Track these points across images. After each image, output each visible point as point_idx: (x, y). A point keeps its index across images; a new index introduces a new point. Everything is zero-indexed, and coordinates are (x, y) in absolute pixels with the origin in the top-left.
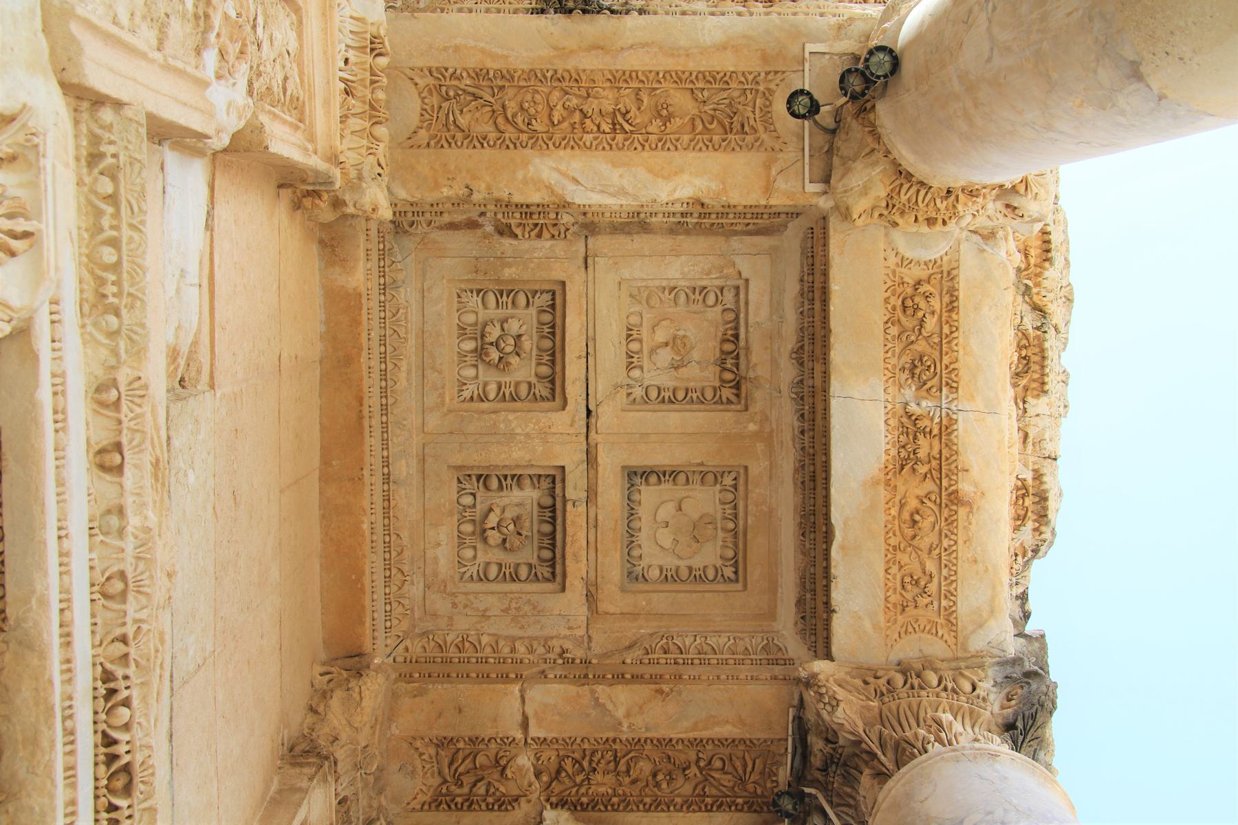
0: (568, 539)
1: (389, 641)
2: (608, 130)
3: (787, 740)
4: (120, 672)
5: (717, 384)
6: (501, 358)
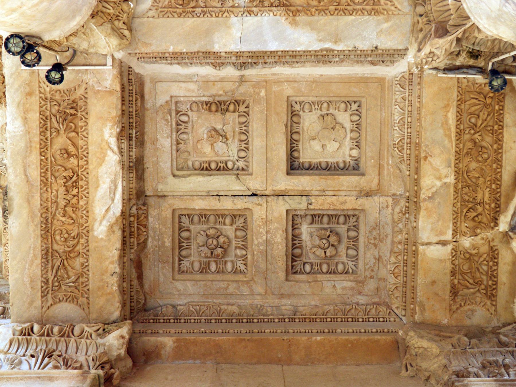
0: (332, 207)
1: (392, 319)
2: (77, 190)
3: (458, 78)
5: (237, 114)
6: (221, 247)
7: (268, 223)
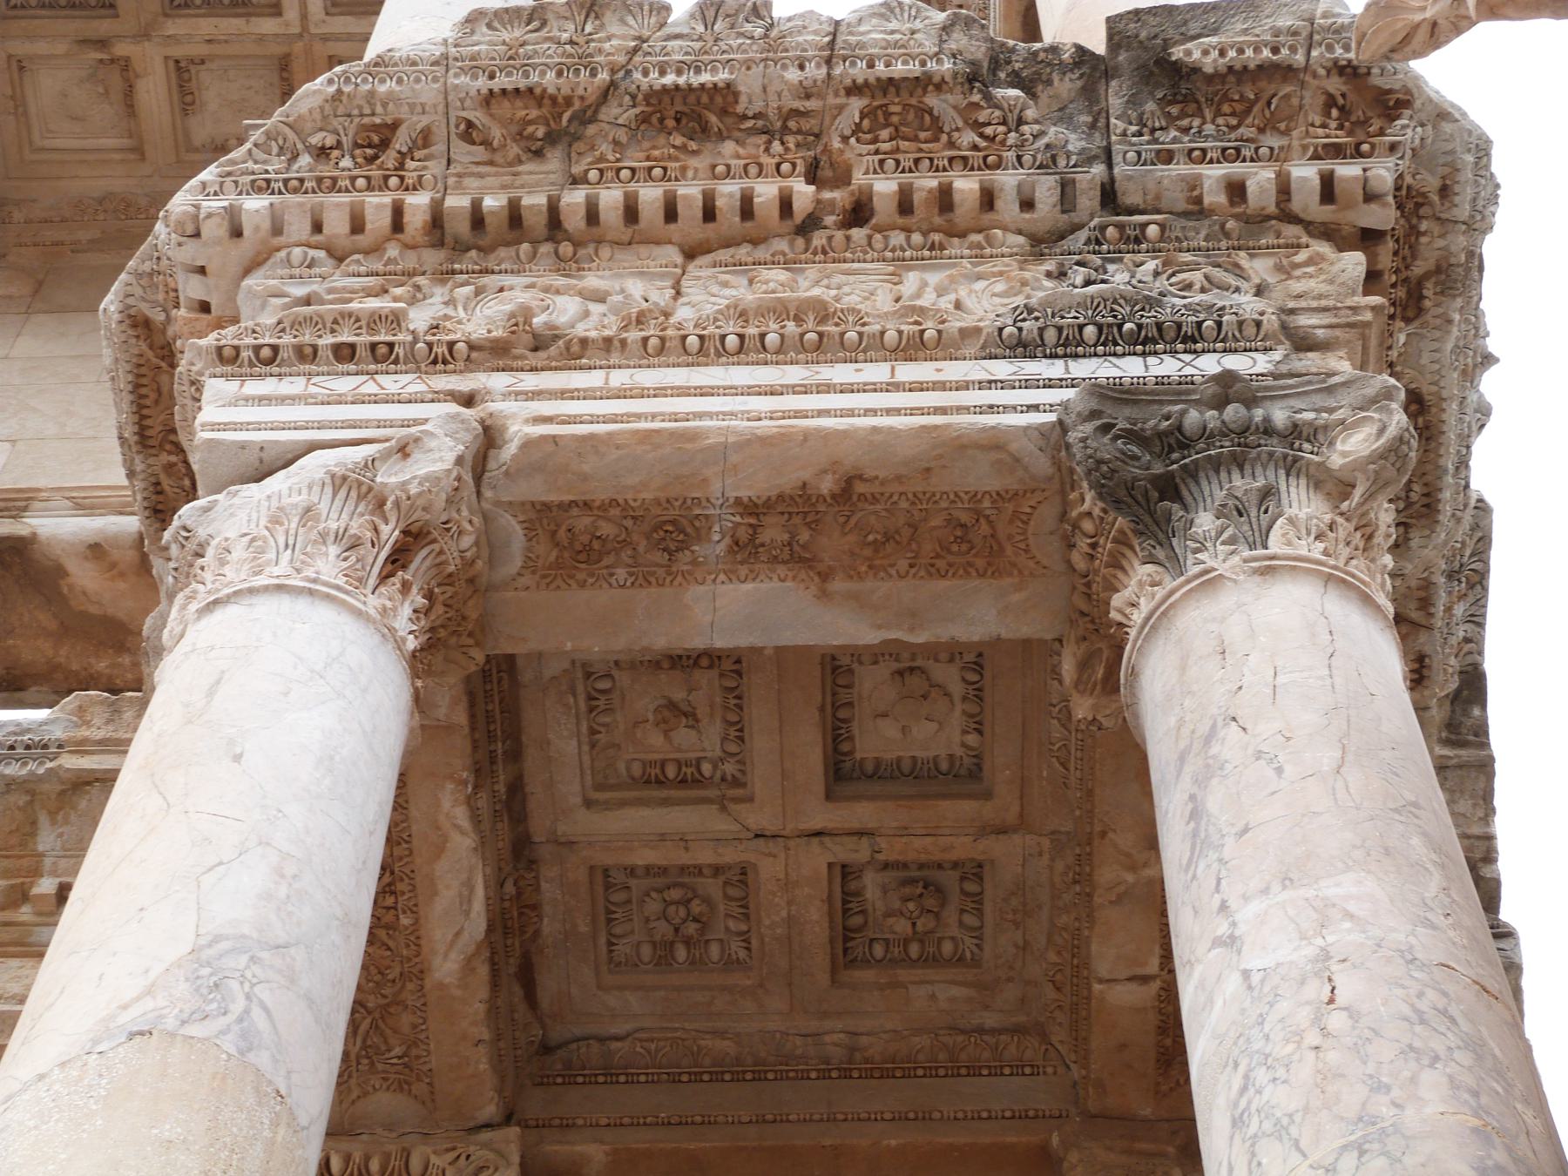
6: (696, 920)
7: (793, 889)
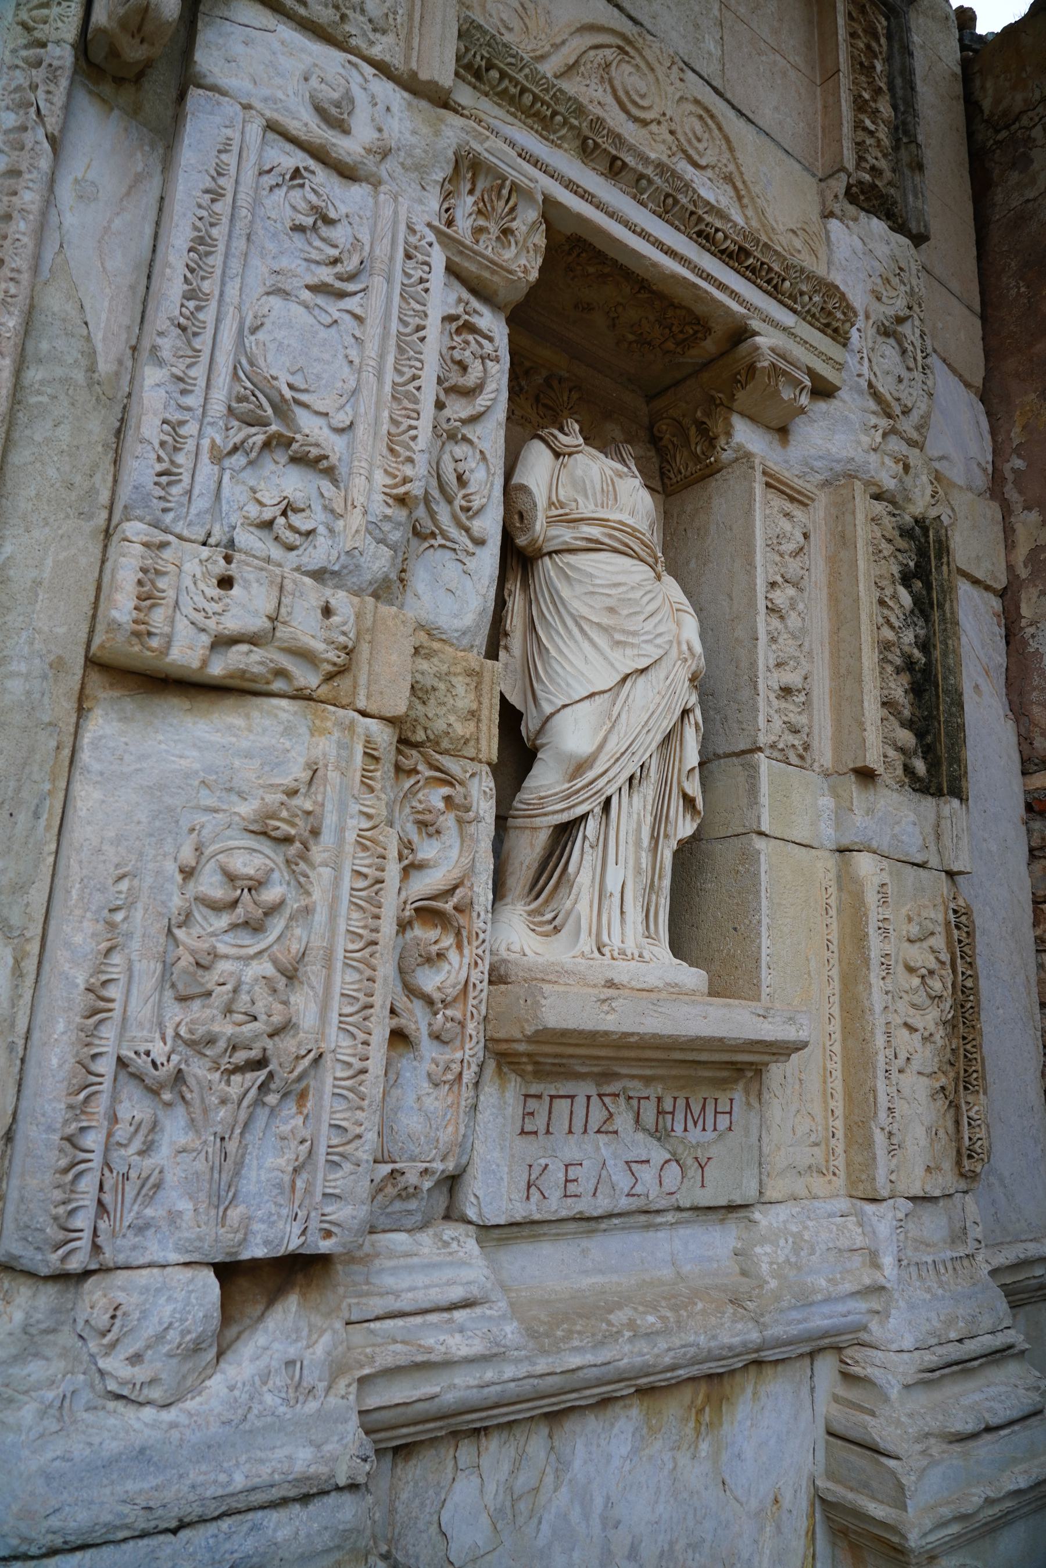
4: (702, 226)
